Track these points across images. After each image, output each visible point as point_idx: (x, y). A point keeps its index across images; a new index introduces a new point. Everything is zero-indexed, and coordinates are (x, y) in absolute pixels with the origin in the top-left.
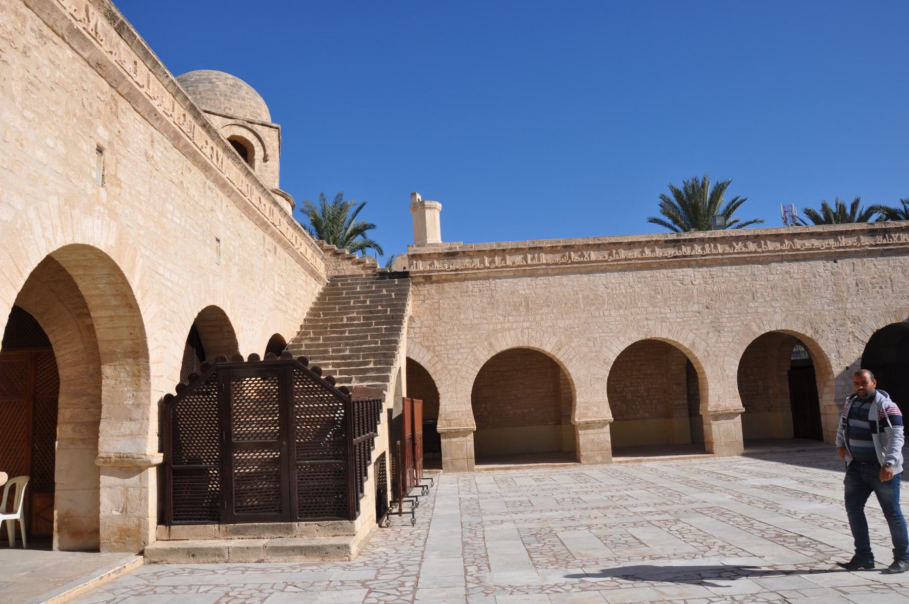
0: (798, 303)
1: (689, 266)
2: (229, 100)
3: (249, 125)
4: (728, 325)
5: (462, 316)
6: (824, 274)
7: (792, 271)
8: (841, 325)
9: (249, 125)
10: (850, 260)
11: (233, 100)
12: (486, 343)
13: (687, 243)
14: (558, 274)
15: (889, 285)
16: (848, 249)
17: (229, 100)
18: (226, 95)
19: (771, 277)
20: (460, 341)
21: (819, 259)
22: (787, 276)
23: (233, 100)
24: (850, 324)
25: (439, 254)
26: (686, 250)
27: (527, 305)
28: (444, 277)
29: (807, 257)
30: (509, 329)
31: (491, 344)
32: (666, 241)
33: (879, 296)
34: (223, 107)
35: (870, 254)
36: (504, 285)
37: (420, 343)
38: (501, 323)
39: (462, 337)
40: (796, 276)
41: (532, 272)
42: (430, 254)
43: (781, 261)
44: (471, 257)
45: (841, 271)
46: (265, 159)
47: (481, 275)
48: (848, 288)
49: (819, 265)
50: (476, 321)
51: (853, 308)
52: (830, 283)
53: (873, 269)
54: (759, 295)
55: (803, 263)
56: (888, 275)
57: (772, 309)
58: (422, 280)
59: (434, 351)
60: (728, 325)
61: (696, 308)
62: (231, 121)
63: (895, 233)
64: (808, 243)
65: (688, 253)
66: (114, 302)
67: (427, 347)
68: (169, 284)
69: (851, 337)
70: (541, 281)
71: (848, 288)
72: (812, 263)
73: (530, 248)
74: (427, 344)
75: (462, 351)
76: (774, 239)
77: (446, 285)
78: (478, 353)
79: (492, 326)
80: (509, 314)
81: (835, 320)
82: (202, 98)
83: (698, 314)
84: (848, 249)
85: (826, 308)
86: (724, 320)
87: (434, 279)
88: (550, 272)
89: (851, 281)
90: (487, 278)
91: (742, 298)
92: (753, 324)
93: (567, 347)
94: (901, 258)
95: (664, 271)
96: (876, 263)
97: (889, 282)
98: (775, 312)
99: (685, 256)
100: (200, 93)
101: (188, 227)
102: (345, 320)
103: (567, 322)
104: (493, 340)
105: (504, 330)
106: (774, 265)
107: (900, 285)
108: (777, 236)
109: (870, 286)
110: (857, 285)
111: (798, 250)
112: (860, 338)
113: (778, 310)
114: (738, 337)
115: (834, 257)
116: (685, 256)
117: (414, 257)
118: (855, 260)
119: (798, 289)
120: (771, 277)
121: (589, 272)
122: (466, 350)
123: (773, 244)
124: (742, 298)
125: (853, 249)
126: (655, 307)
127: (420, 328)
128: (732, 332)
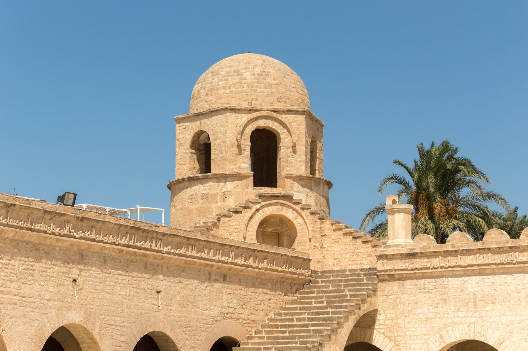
2: (255, 91)
3: (275, 115)
5: (419, 311)
11: (259, 90)
12: (438, 336)
17: (255, 91)
18: (253, 87)
20: (416, 333)
23: (259, 90)
25: (401, 254)
27: (475, 302)
28: (405, 276)
30: (458, 324)
31: (442, 337)
34: (250, 99)
36: (454, 283)
37: (384, 334)
38: (451, 318)
39: (418, 329)
42: (393, 255)
47: (436, 274)
50: (431, 316)
58: (388, 278)
59: (395, 341)
62: (255, 114)
66: (88, 341)
67: (389, 337)
68: (119, 328)
70: (487, 280)
73: (479, 249)
74: (389, 334)
75: (418, 341)
77: (407, 282)
78: (431, 344)
79: (443, 320)
80: (459, 310)
82: (231, 92)
87: (396, 277)
88: (496, 271)
90: (442, 276)
93: (508, 342)
100: (229, 88)
101: (132, 293)
102: (295, 320)
103: (510, 318)
104: (444, 333)
105: (454, 324)
117: (380, 257)
122: (420, 341)
127: (385, 320)
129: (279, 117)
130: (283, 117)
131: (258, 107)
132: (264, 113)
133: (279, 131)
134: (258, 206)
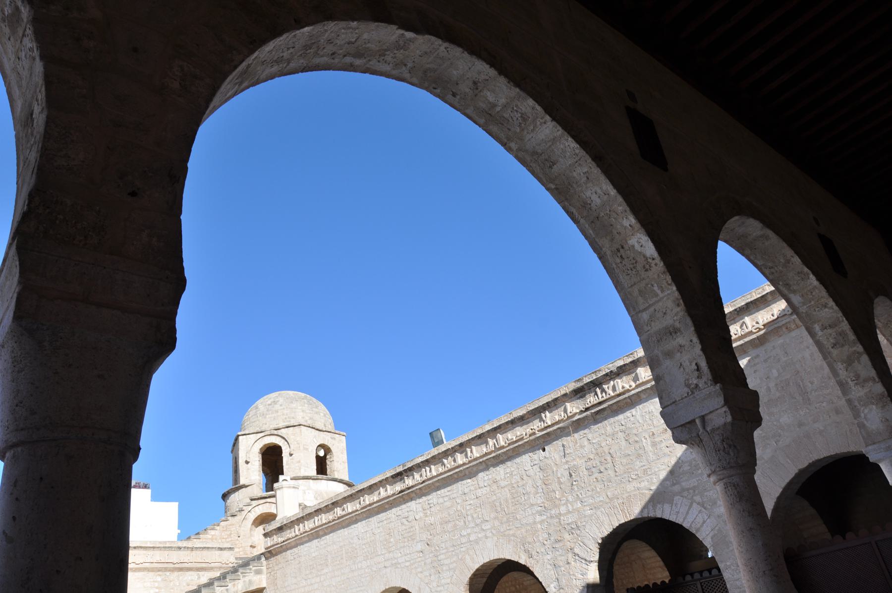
0: (508, 521)
1: (412, 500)
3: (276, 432)
4: (447, 562)
6: (531, 473)
7: (498, 479)
8: (557, 541)
9: (276, 432)
10: (559, 443)
13: (409, 473)
14: (331, 532)
15: (610, 465)
16: (549, 430)
19: (479, 492)
21: (524, 453)
22: (495, 487)
24: (567, 536)
26: (409, 482)
29: (510, 454)
32: (392, 477)
33: (599, 486)
35: (578, 425)
40: (503, 483)
41: (316, 534)
43: (487, 468)
44: (290, 528)
45: (549, 462)
46: (291, 455)
48: (560, 483)
49: (525, 460)
51: (569, 512)
52: (539, 483)
53: (588, 447)
54: (470, 518)
55: (509, 463)
56: (606, 449)
57: (483, 534)
60: (447, 562)
61: (419, 547)
63: (608, 382)
64: (511, 435)
65: (411, 484)
69: (570, 555)
71: (560, 483)
72: (518, 460)
76: (479, 441)
81: (549, 534)
83: (421, 554)
84: (549, 430)
85: (538, 518)
86: (442, 557)
89: (563, 473)
90: (296, 546)
91: (455, 526)
92: (467, 557)
94: (621, 417)
95: (394, 510)
96: (590, 436)
97: (609, 458)
98: (486, 537)
99: (409, 488)
106: (481, 475)
107: (624, 461)
108: (480, 437)
109: (586, 472)
110: (571, 475)
111: (503, 447)
112: (582, 554)
113: (489, 534)
114: (455, 577)
115: (540, 443)
116: (409, 488)
118: (566, 440)
119: (507, 501)
120: (479, 492)
121: (348, 525)
123: (479, 448)
124: (455, 526)
125: (555, 427)
126: (390, 552)
128: (450, 569)
129: (279, 432)
130: (283, 432)
131: (263, 429)
132: (268, 433)
133: (280, 444)
134: (250, 508)
